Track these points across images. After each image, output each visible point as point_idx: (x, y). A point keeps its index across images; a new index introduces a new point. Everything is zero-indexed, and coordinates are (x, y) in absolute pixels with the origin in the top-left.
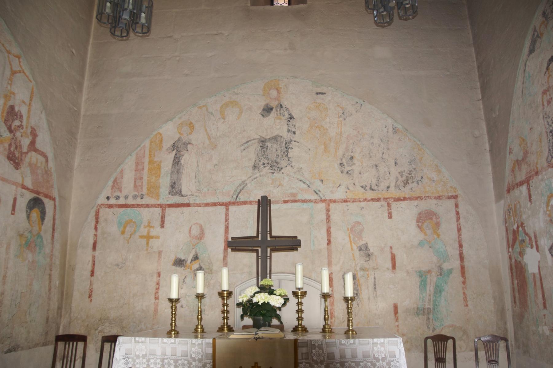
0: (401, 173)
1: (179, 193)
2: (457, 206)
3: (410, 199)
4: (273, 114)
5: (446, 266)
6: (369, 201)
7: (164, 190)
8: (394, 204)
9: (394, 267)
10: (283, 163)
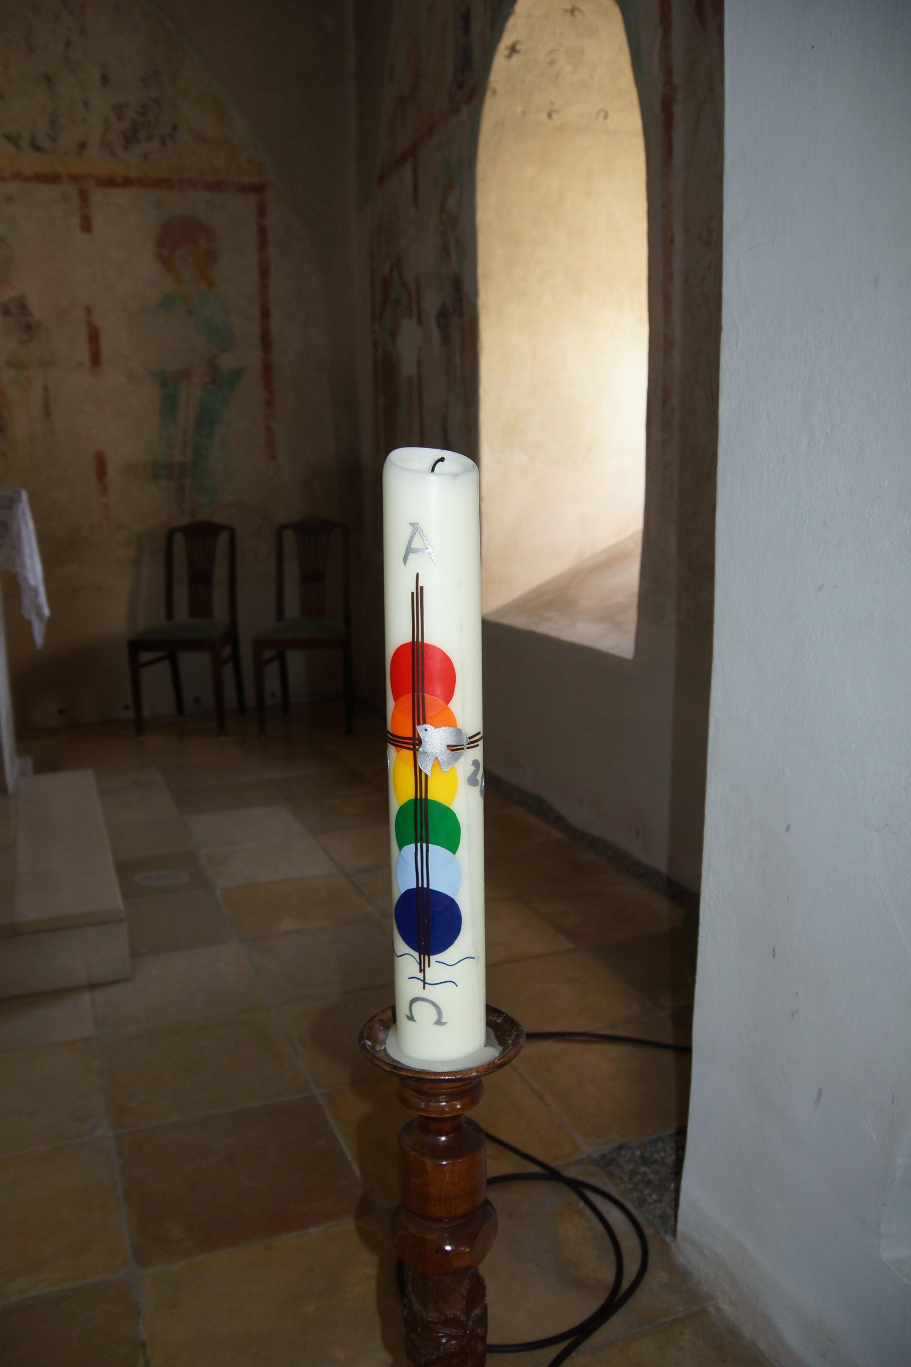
0: (119, 110)
2: (261, 212)
3: (142, 183)
5: (227, 362)
6: (27, 179)
8: (98, 196)
9: (96, 359)
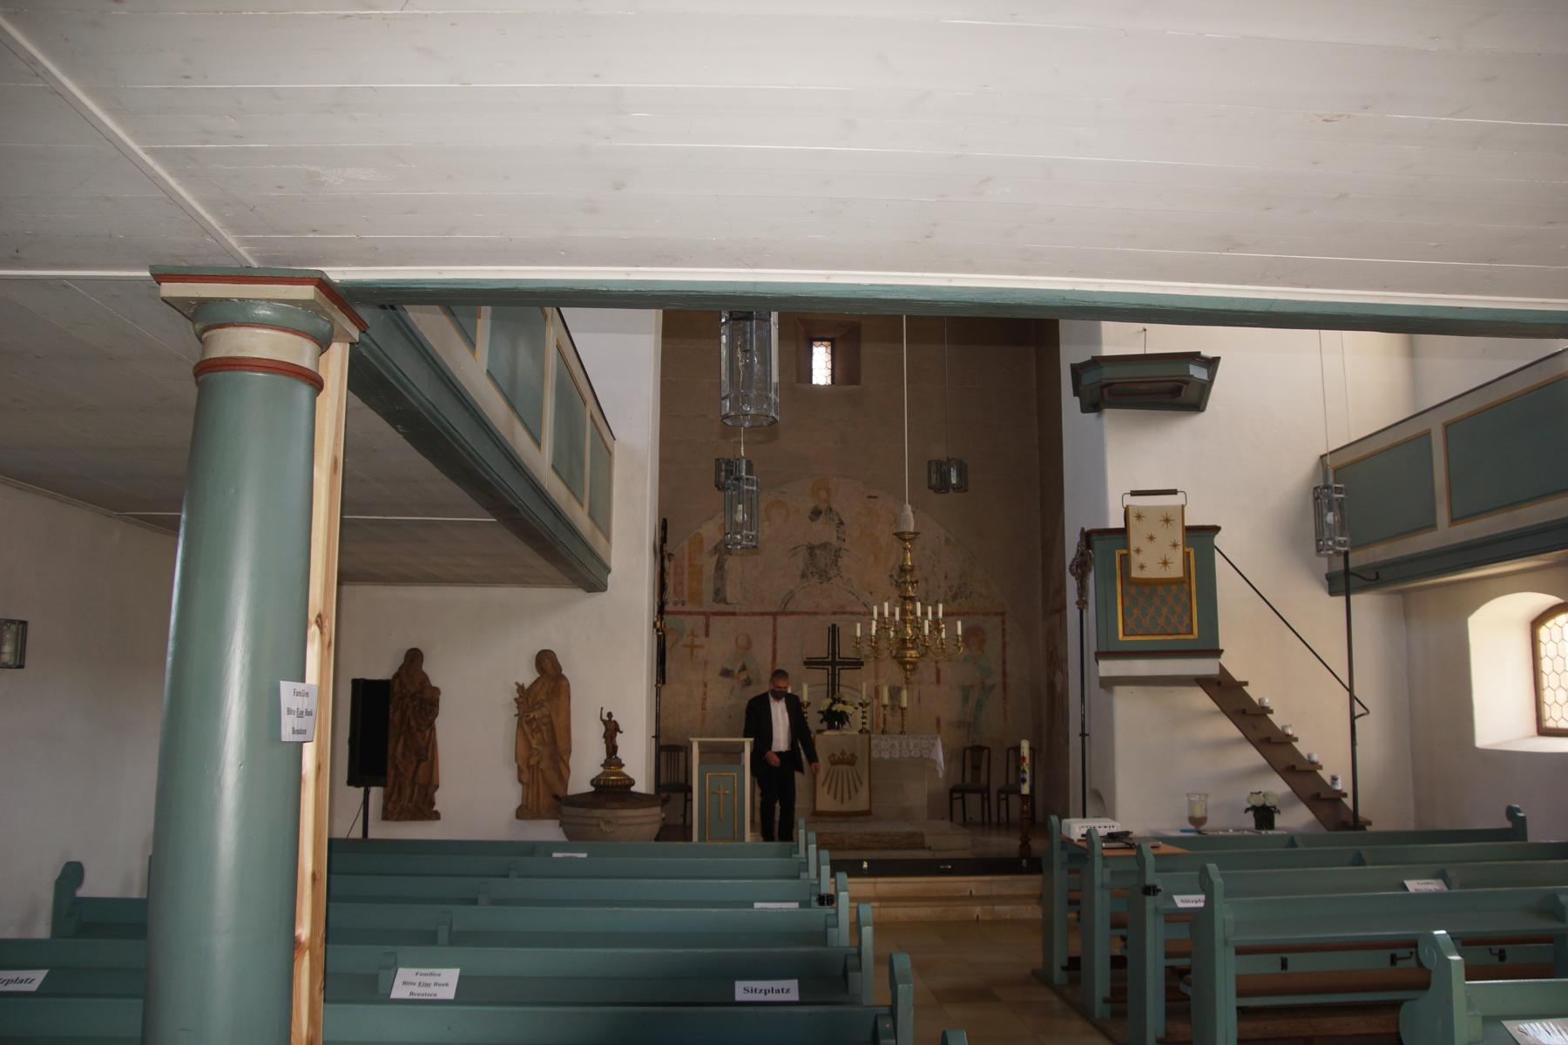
0: (950, 588)
1: (724, 601)
2: (1003, 622)
4: (822, 518)
7: (708, 596)
9: (938, 681)
10: (832, 573)
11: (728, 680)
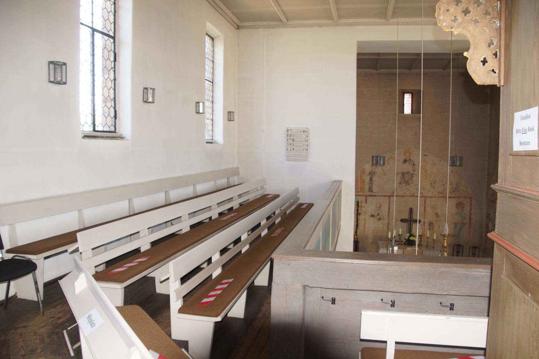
0: (453, 188)
1: (372, 191)
3: (455, 197)
4: (407, 163)
5: (464, 221)
7: (366, 189)
10: (410, 182)
11: (372, 218)
